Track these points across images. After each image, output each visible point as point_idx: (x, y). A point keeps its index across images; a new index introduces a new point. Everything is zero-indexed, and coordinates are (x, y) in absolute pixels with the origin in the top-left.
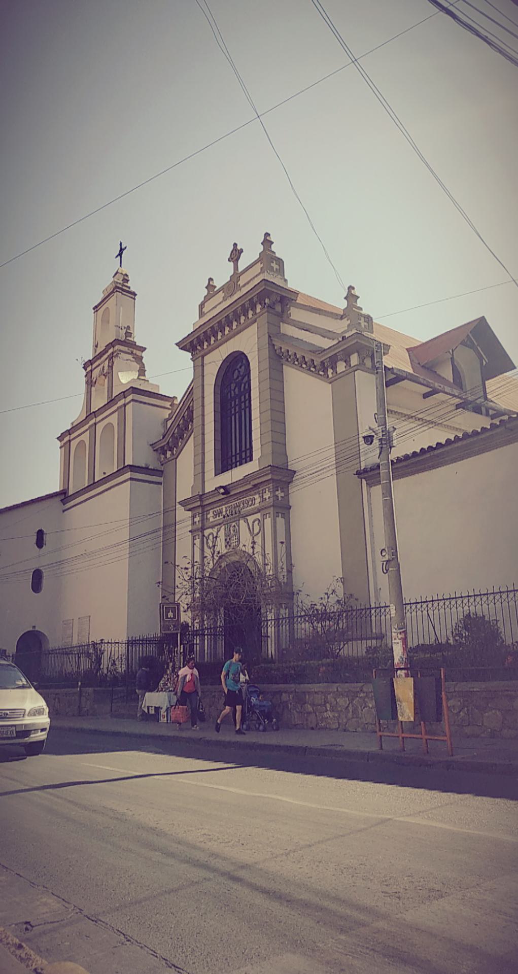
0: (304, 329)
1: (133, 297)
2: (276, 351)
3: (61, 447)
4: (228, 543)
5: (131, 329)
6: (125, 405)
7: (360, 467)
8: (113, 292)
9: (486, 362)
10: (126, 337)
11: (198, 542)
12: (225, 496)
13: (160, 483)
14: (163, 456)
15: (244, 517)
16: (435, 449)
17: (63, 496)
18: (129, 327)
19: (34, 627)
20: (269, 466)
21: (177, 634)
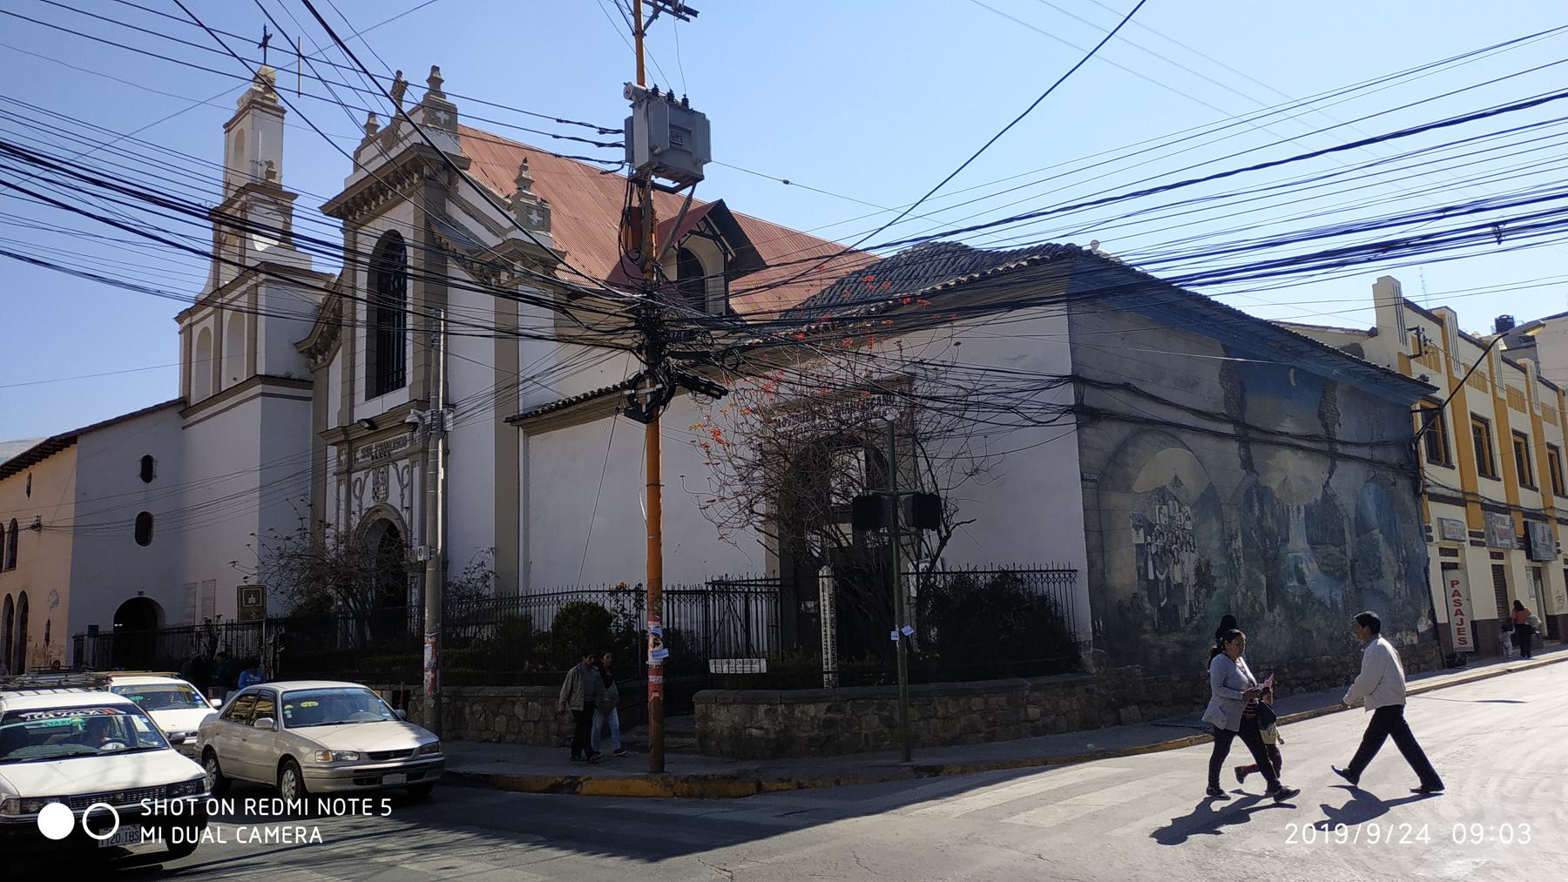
0: (469, 214)
1: (281, 114)
2: (435, 239)
3: (180, 333)
4: (376, 493)
5: (274, 166)
6: (256, 286)
7: (518, 411)
8: (247, 108)
9: (731, 254)
10: (268, 178)
11: (343, 488)
12: (372, 432)
13: (309, 399)
14: (312, 360)
15: (394, 462)
16: (575, 403)
17: (182, 407)
18: (270, 164)
19: (141, 593)
20: (416, 400)
21: (262, 623)
